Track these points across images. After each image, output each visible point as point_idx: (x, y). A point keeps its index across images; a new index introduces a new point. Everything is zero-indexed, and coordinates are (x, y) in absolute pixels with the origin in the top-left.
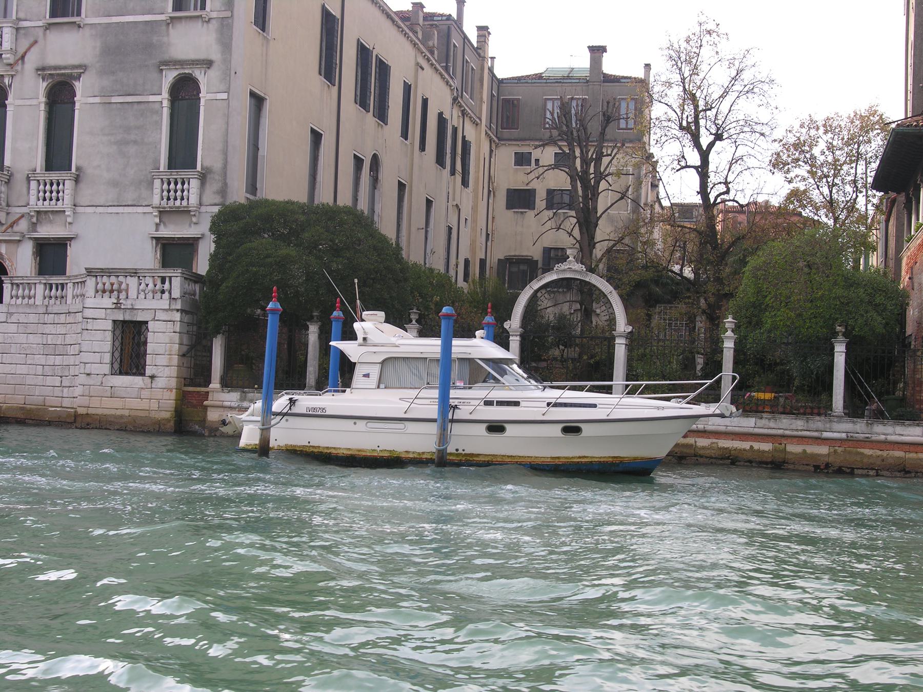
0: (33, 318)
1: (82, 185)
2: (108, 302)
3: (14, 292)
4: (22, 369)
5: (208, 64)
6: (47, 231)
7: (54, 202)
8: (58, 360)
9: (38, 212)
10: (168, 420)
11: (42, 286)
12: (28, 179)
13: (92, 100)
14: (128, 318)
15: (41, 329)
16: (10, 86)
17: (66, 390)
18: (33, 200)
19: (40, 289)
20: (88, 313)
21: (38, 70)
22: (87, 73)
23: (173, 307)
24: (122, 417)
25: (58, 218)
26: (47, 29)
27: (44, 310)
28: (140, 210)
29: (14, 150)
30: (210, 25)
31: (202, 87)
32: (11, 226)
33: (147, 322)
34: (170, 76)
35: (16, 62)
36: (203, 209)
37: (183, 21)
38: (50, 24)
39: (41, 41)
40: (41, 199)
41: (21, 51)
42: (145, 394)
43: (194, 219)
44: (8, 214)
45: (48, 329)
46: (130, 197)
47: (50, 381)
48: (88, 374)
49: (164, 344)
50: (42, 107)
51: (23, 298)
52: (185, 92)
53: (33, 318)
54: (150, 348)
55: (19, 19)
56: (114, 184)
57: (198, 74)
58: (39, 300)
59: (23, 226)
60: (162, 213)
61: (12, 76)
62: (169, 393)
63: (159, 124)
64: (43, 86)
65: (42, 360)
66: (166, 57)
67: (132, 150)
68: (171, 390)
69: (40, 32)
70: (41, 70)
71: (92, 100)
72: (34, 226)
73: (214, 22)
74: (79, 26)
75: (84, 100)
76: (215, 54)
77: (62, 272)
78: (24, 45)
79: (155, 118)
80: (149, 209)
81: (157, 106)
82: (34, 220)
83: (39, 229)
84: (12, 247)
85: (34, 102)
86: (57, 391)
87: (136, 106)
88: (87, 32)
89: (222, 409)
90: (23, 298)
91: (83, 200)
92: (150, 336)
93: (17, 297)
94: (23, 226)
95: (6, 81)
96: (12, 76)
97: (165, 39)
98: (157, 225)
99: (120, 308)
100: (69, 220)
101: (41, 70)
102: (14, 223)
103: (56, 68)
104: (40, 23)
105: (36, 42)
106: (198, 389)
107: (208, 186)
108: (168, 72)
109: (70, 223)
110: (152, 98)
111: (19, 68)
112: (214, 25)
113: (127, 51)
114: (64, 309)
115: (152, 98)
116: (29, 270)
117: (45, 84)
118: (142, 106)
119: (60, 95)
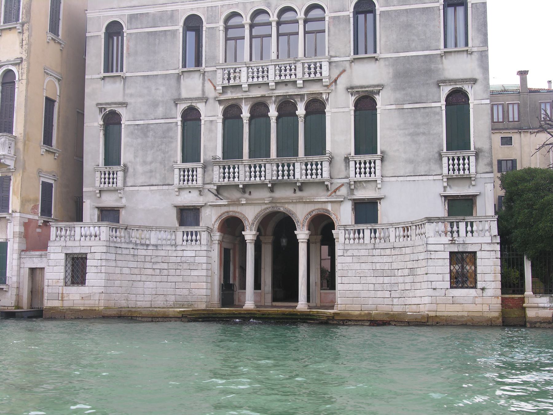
0: (363, 252)
1: (386, 163)
2: (446, 239)
3: (347, 236)
4: (359, 287)
5: (474, 81)
6: (361, 194)
7: (368, 175)
8: (386, 280)
9: (355, 182)
10: (497, 318)
11: (369, 231)
14: (461, 250)
15: (370, 259)
16: (327, 100)
17: (395, 300)
18: (352, 174)
19: (179, 234)
20: (430, 248)
21: (347, 89)
22: (384, 89)
23: (494, 241)
24: (462, 317)
25: (369, 185)
26: (352, 62)
28: (431, 178)
29: (332, 141)
30: (473, 56)
31: (470, 96)
32: (335, 192)
33: (475, 253)
34: (446, 90)
35: (331, 84)
36: (478, 176)
37: (453, 54)
38: (354, 59)
40: (358, 173)
41: (334, 77)
42: (479, 300)
43: (473, 183)
44: (331, 184)
45: (376, 259)
46: (422, 169)
47: (379, 294)
48: (434, 289)
49: (489, 267)
50: (352, 113)
51: (354, 239)
55: (331, 57)
56: (410, 161)
59: (344, 191)
60: (450, 179)
61: (329, 93)
62: (496, 299)
63: (440, 121)
64: (352, 100)
65: (373, 280)
66: (442, 78)
67: (422, 139)
68: (498, 297)
69: (347, 65)
70: (350, 89)
72: (352, 191)
73: (475, 54)
74: (377, 60)
75: (384, 107)
76: (477, 74)
77: (375, 220)
79: (437, 117)
80: (440, 177)
81: (438, 110)
82: (353, 187)
83: (355, 193)
84: (336, 206)
85: (347, 110)
87: (422, 110)
88: (382, 63)
89: (537, 309)
90: (354, 239)
91: (388, 173)
93: (349, 239)
94: (344, 191)
95: (324, 96)
96: (329, 93)
97: (440, 66)
98: (445, 187)
99: (455, 243)
100: (379, 186)
101: (350, 89)
102: (337, 189)
103: (362, 87)
104: (348, 59)
105: (344, 71)
106: (513, 296)
107: (480, 160)
108: (444, 87)
109: (379, 189)
110: (434, 105)
111: (333, 87)
112: (475, 56)
114: (389, 245)
115: (434, 105)
116: (350, 220)
117: (353, 98)
118: (427, 110)
119: (365, 105)
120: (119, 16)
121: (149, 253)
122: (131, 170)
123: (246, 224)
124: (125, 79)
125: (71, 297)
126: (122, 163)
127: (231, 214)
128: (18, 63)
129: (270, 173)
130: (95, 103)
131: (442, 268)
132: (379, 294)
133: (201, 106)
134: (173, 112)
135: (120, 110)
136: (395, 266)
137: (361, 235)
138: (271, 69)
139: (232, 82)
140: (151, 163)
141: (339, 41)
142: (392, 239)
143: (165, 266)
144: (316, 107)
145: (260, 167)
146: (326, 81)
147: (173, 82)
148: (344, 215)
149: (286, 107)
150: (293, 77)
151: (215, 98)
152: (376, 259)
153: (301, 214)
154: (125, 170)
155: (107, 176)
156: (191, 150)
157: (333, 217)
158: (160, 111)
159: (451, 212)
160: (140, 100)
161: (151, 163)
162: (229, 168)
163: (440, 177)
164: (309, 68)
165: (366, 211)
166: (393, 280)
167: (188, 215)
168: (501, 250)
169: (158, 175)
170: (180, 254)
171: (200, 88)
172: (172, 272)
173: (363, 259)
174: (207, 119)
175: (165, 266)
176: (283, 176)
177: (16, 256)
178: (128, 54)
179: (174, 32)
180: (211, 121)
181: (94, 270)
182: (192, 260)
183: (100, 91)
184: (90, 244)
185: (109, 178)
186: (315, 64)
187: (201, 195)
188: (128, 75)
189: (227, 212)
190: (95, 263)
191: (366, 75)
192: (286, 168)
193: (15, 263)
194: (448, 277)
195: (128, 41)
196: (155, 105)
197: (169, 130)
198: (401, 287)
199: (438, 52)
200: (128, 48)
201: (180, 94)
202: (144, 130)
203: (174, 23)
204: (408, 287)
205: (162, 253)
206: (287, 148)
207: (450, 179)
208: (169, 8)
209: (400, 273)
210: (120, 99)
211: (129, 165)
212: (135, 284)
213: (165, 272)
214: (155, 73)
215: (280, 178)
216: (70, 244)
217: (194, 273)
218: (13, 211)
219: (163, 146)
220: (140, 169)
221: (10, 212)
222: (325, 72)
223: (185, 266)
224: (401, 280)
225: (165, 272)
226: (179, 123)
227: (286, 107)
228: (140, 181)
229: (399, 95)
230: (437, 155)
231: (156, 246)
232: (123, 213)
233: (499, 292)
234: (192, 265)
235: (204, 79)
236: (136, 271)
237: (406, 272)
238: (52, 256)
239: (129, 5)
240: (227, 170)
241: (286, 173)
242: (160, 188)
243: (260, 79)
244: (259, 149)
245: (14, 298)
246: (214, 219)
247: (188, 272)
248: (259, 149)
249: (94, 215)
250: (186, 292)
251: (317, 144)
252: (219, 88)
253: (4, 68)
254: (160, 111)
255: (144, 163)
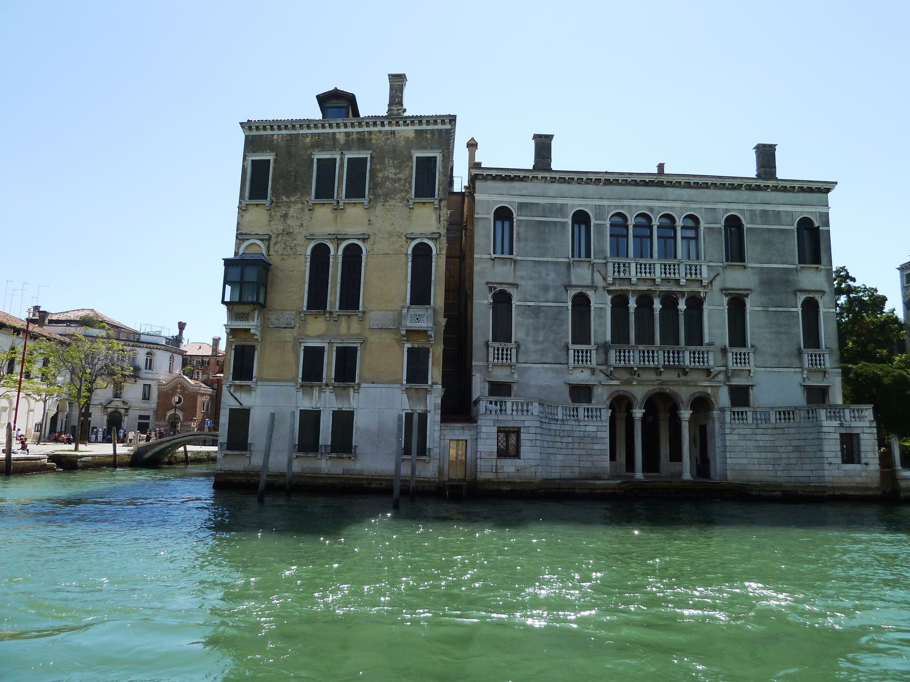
0: (748, 431)
2: (836, 423)
4: (745, 461)
5: (822, 292)
6: (736, 382)
8: (769, 455)
12: (724, 351)
13: (756, 309)
14: (848, 432)
21: (722, 290)
27: (754, 426)
28: (792, 370)
33: (858, 434)
34: (802, 297)
39: (722, 274)
42: (864, 474)
45: (758, 437)
47: (763, 467)
48: (830, 464)
50: (726, 311)
52: (811, 307)
53: (748, 431)
54: (863, 448)
57: (817, 297)
58: (750, 420)
64: (726, 300)
65: (758, 455)
66: (798, 287)
69: (721, 270)
71: (756, 309)
72: (728, 378)
74: (745, 267)
78: (713, 276)
85: (721, 308)
86: (772, 474)
88: (749, 271)
92: (862, 442)
94: (721, 377)
97: (796, 278)
105: (718, 274)
110: (793, 309)
113: (776, 284)
115: (793, 309)
119: (737, 304)
120: (509, 203)
121: (558, 427)
122: (522, 348)
123: (635, 403)
124: (515, 261)
125: (506, 470)
126: (513, 340)
127: (621, 393)
128: (436, 238)
129: (660, 359)
130: (485, 281)
131: (832, 448)
132: (763, 467)
133: (590, 293)
134: (564, 297)
135: (510, 290)
136: (777, 443)
137: (745, 416)
138: (658, 267)
139: (622, 275)
140: (543, 342)
141: (713, 249)
142: (773, 420)
143: (570, 440)
144: (696, 303)
145: (653, 352)
146: (705, 282)
147: (563, 269)
148: (723, 398)
149: (669, 300)
150: (677, 275)
151: (604, 288)
152: (758, 437)
153: (685, 394)
154: (518, 348)
155: (500, 352)
156: (581, 333)
157: (713, 399)
158: (551, 294)
159: (809, 400)
160: (531, 282)
161: (543, 342)
162: (624, 352)
163: (799, 370)
164: (690, 269)
165: (740, 396)
166: (776, 455)
167: (581, 393)
168: (878, 433)
169: (550, 355)
170: (583, 428)
171: (590, 277)
172: (576, 445)
173: (748, 437)
174: (597, 306)
175: (570, 440)
176: (674, 362)
177: (437, 428)
178: (519, 239)
179: (564, 224)
180: (601, 308)
181: (529, 443)
182: (593, 435)
183: (487, 271)
184: (523, 418)
185: (503, 354)
186: (696, 267)
187: (593, 374)
188: (518, 258)
189: (618, 391)
190: (530, 437)
191: (737, 278)
192: (676, 355)
193: (437, 434)
194: (839, 454)
195: (518, 226)
196: (546, 288)
197: (560, 313)
198: (786, 461)
199: (794, 266)
200: (518, 234)
201: (570, 281)
202: (536, 311)
203: (564, 215)
204: (793, 461)
205: (568, 428)
206: (670, 337)
207: (809, 371)
208: (559, 201)
209: (783, 449)
210: (511, 281)
211: (520, 342)
212: (553, 457)
213: (570, 446)
214: (546, 259)
215: (672, 363)
216: (501, 417)
217: (597, 447)
218: (433, 383)
219: (555, 328)
220: (532, 347)
221: (430, 383)
222: (705, 274)
223: (588, 440)
224: (784, 455)
225: (570, 446)
226: (570, 308)
227: (669, 300)
228: (533, 358)
229: (764, 299)
230: (796, 352)
231: (563, 421)
232: (515, 387)
233: (878, 467)
234: (594, 439)
235: (593, 269)
236: (550, 444)
237: (790, 449)
238: (484, 429)
239: (519, 193)
240: (622, 354)
241: (671, 359)
242: (553, 366)
243: (648, 275)
244: (645, 337)
245: (436, 469)
246: (605, 398)
247: (590, 446)
248: (645, 337)
249: (484, 388)
250: (589, 464)
251: (695, 336)
252: (610, 280)
253: (417, 241)
254: (551, 294)
255: (536, 342)
